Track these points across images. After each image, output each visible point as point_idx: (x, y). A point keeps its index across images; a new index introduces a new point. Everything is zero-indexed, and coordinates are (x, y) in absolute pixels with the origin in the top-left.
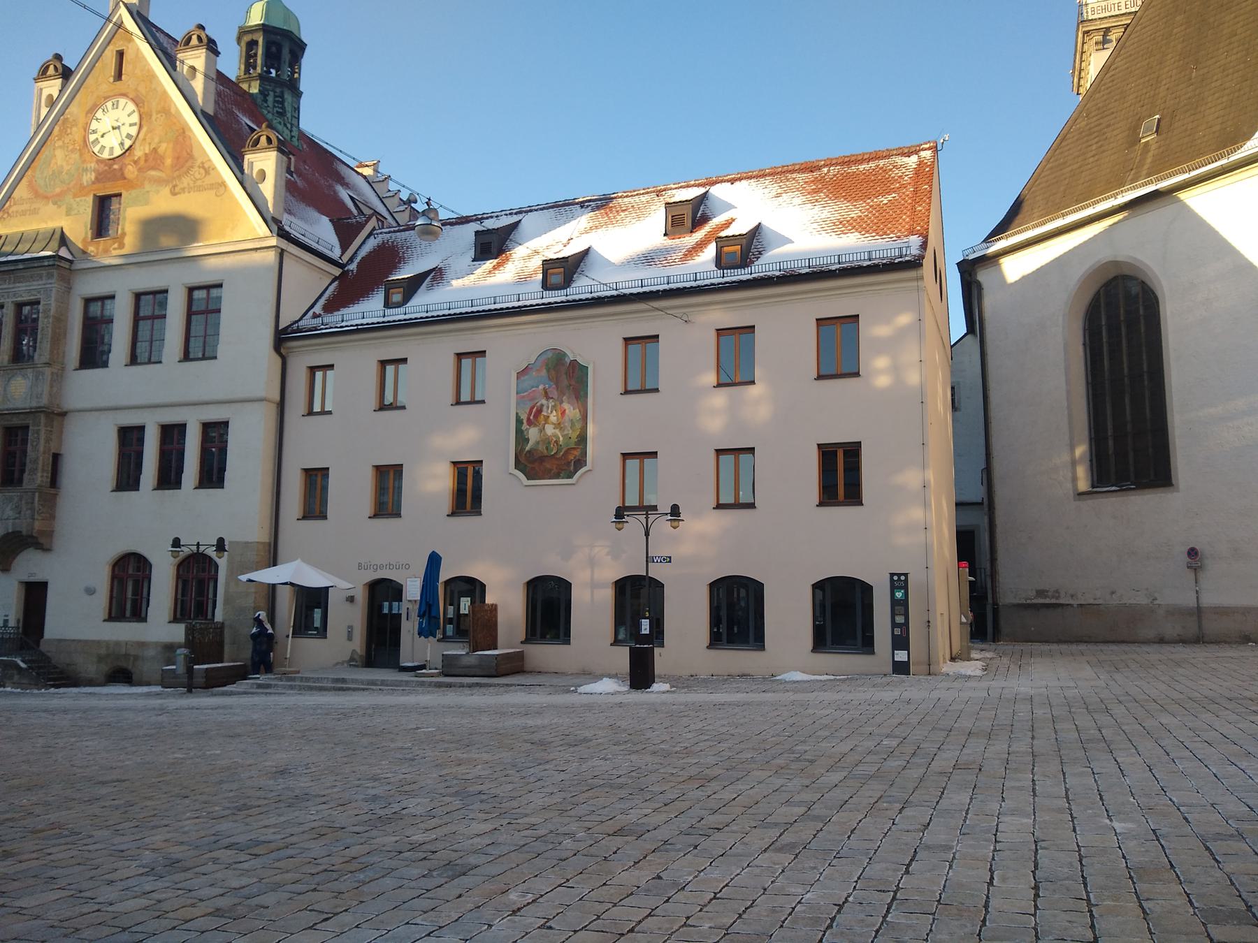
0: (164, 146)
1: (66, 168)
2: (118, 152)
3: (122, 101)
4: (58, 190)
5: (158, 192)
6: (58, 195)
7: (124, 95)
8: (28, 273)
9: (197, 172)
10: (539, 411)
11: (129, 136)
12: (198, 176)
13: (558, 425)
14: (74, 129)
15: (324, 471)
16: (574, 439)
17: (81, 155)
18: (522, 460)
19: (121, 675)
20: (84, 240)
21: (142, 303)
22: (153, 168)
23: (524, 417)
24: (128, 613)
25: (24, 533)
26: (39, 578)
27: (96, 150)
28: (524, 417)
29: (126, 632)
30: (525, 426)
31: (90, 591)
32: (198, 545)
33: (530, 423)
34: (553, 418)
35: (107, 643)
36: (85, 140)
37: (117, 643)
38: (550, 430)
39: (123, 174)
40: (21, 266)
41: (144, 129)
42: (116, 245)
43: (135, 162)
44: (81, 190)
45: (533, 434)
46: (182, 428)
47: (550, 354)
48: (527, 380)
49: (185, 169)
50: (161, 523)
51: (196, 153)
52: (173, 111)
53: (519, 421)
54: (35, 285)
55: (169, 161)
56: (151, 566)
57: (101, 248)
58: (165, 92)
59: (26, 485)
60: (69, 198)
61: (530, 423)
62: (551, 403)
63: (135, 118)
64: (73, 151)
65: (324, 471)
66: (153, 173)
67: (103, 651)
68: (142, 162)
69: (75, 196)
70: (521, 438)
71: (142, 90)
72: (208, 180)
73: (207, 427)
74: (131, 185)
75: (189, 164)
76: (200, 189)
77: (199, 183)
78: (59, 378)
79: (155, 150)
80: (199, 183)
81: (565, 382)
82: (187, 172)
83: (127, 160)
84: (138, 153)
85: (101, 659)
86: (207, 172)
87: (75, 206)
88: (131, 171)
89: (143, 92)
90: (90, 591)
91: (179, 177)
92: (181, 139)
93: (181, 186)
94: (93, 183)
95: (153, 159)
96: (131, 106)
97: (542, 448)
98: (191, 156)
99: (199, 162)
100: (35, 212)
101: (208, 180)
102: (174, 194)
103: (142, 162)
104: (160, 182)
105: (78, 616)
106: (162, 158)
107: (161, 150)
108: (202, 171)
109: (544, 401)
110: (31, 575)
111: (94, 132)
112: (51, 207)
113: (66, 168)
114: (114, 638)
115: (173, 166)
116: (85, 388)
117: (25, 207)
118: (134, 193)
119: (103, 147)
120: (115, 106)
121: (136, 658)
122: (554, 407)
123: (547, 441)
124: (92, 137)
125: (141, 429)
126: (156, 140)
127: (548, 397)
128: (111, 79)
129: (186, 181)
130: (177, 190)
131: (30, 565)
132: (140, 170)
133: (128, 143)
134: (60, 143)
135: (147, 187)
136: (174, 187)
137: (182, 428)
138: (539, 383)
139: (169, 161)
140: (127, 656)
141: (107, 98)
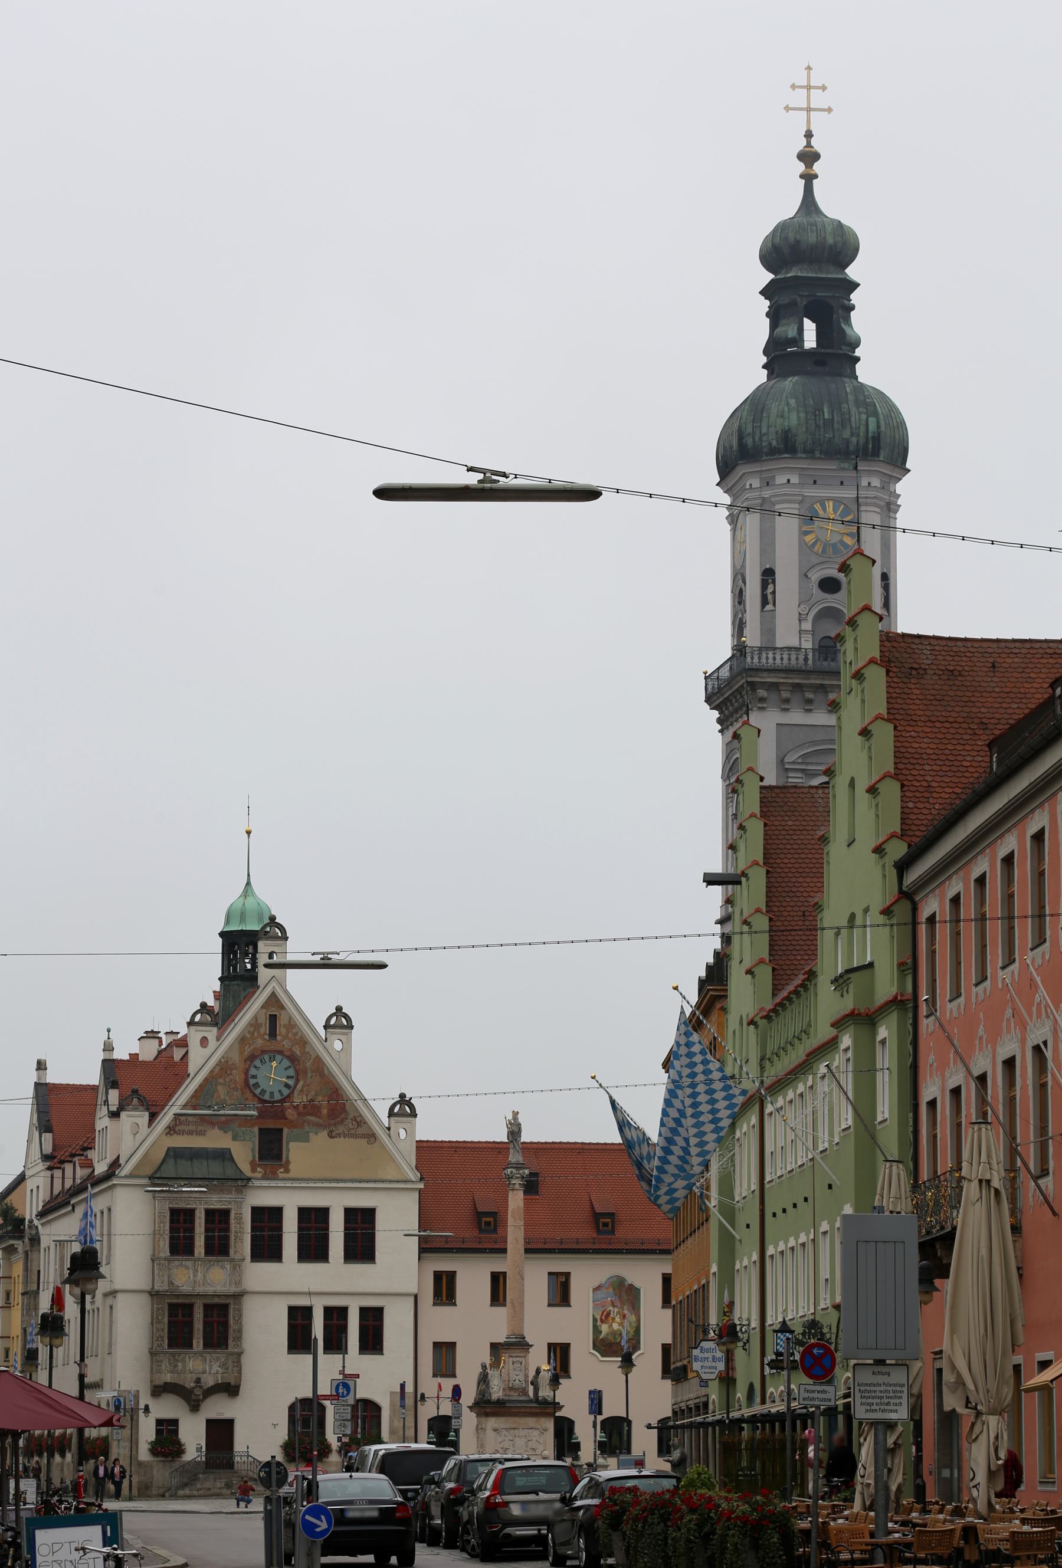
0: (320, 1098)
2: (277, 1097)
3: (279, 1057)
5: (317, 1134)
7: (280, 1052)
10: (608, 1314)
12: (350, 1126)
13: (621, 1324)
14: (235, 1072)
15: (452, 1345)
16: (632, 1333)
17: (243, 1094)
18: (598, 1344)
22: (311, 1114)
23: (598, 1317)
25: (233, 1383)
27: (257, 1091)
28: (598, 1317)
30: (599, 1323)
33: (602, 1321)
34: (618, 1319)
36: (246, 1082)
38: (615, 1326)
41: (301, 1083)
43: (296, 1107)
45: (604, 1328)
47: (615, 1279)
48: (600, 1294)
51: (347, 1107)
52: (326, 1072)
53: (595, 1320)
54: (226, 1197)
55: (325, 1111)
59: (230, 1349)
61: (602, 1321)
62: (616, 1310)
64: (235, 1089)
65: (452, 1345)
66: (312, 1118)
68: (301, 1109)
69: (240, 1126)
70: (596, 1330)
71: (297, 1051)
72: (360, 1131)
73: (364, 1311)
74: (292, 1125)
76: (355, 1136)
77: (353, 1132)
78: (237, 1265)
79: (312, 1100)
81: (626, 1297)
82: (342, 1121)
84: (297, 1100)
86: (359, 1124)
88: (290, 1114)
91: (335, 1124)
94: (258, 1117)
95: (311, 1108)
96: (286, 1063)
97: (611, 1338)
98: (344, 1109)
99: (351, 1116)
100: (202, 1133)
101: (360, 1131)
102: (331, 1137)
103: (301, 1109)
104: (320, 1126)
109: (611, 1308)
111: (254, 1077)
112: (216, 1132)
116: (260, 1275)
117: (191, 1128)
122: (618, 1313)
123: (614, 1333)
124: (252, 1081)
125: (309, 1309)
127: (614, 1306)
128: (267, 1037)
129: (341, 1129)
130: (334, 1134)
131: (218, 1408)
132: (299, 1114)
133: (286, 1092)
134: (221, 1081)
135: (307, 1128)
136: (331, 1131)
138: (608, 1296)
141: (263, 1052)
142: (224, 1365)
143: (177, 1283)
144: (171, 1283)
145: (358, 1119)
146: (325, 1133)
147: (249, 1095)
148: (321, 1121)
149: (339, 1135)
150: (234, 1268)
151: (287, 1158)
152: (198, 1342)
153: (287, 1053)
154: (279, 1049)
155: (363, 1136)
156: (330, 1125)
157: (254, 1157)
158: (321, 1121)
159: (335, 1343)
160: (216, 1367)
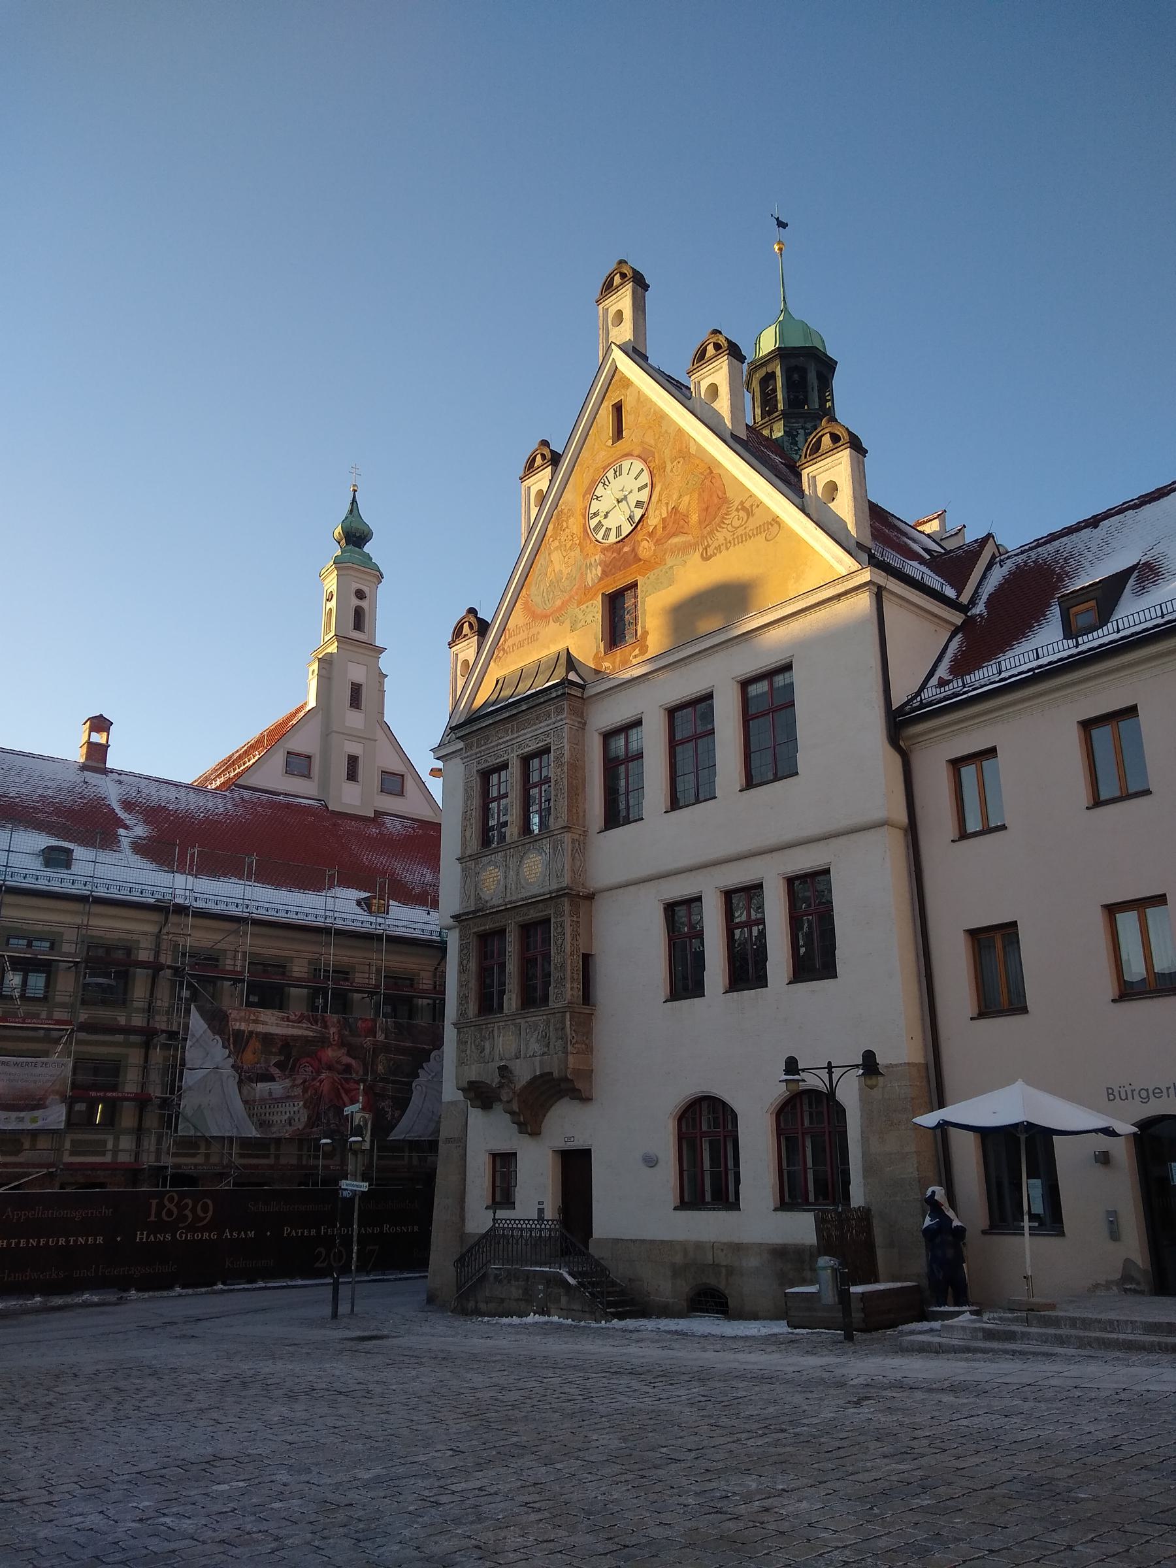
0: (686, 499)
1: (565, 572)
2: (627, 529)
3: (626, 464)
4: (558, 603)
6: (560, 608)
8: (531, 715)
9: (735, 518)
11: (639, 504)
12: (736, 523)
14: (571, 520)
19: (710, 1300)
20: (596, 656)
21: (678, 721)
22: (674, 535)
24: (708, 1198)
26: (578, 1144)
27: (599, 537)
29: (707, 1227)
31: (651, 1162)
32: (830, 1067)
35: (683, 1246)
37: (699, 1246)
39: (636, 555)
40: (524, 707)
42: (637, 652)
43: (651, 535)
44: (586, 593)
46: (754, 890)
49: (717, 520)
50: (744, 1047)
52: (693, 450)
54: (542, 727)
55: (694, 518)
56: (735, 1116)
57: (618, 660)
58: (680, 431)
59: (552, 1003)
60: (573, 610)
63: (645, 478)
66: (675, 540)
67: (678, 1259)
68: (659, 531)
69: (579, 604)
72: (753, 523)
74: (648, 566)
75: (723, 511)
76: (742, 539)
77: (740, 531)
78: (581, 846)
80: (740, 531)
83: (640, 535)
84: (653, 521)
85: (677, 1272)
86: (749, 513)
87: (580, 616)
88: (646, 548)
89: (652, 442)
90: (651, 1162)
91: (711, 533)
92: (707, 482)
93: (716, 544)
94: (601, 579)
95: (676, 521)
98: (724, 500)
99: (736, 503)
100: (533, 639)
101: (753, 523)
102: (706, 558)
104: (686, 548)
105: (637, 1204)
106: (685, 517)
107: (682, 508)
108: (742, 513)
110: (570, 1139)
111: (595, 515)
112: (553, 626)
113: (565, 572)
114: (694, 1236)
115: (700, 522)
116: (616, 855)
117: (523, 635)
118: (652, 575)
119: (608, 530)
120: (618, 473)
121: (731, 1271)
126: (675, 497)
129: (720, 536)
130: (710, 552)
131: (567, 1125)
132: (658, 543)
134: (556, 543)
135: (670, 563)
137: (754, 890)
139: (694, 518)
140: (716, 1266)
141: (606, 468)
142: (545, 1040)
143: (486, 894)
144: (478, 898)
145: (747, 505)
146: (697, 555)
147: (590, 548)
148: (689, 538)
149: (719, 549)
150: (555, 849)
151: (643, 627)
152: (511, 1001)
153: (636, 453)
154: (627, 451)
155: (758, 531)
156: (704, 537)
157: (598, 647)
158: (689, 538)
159: (747, 971)
160: (535, 1047)
